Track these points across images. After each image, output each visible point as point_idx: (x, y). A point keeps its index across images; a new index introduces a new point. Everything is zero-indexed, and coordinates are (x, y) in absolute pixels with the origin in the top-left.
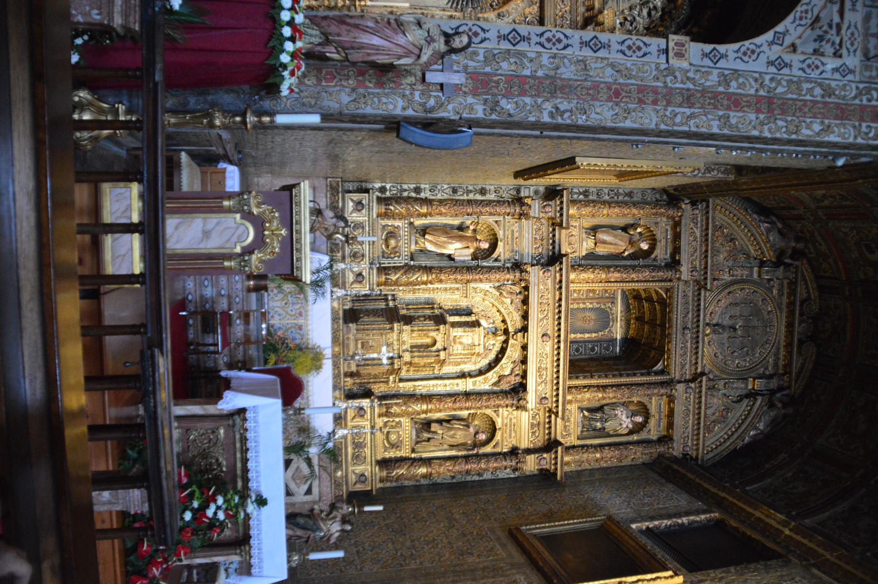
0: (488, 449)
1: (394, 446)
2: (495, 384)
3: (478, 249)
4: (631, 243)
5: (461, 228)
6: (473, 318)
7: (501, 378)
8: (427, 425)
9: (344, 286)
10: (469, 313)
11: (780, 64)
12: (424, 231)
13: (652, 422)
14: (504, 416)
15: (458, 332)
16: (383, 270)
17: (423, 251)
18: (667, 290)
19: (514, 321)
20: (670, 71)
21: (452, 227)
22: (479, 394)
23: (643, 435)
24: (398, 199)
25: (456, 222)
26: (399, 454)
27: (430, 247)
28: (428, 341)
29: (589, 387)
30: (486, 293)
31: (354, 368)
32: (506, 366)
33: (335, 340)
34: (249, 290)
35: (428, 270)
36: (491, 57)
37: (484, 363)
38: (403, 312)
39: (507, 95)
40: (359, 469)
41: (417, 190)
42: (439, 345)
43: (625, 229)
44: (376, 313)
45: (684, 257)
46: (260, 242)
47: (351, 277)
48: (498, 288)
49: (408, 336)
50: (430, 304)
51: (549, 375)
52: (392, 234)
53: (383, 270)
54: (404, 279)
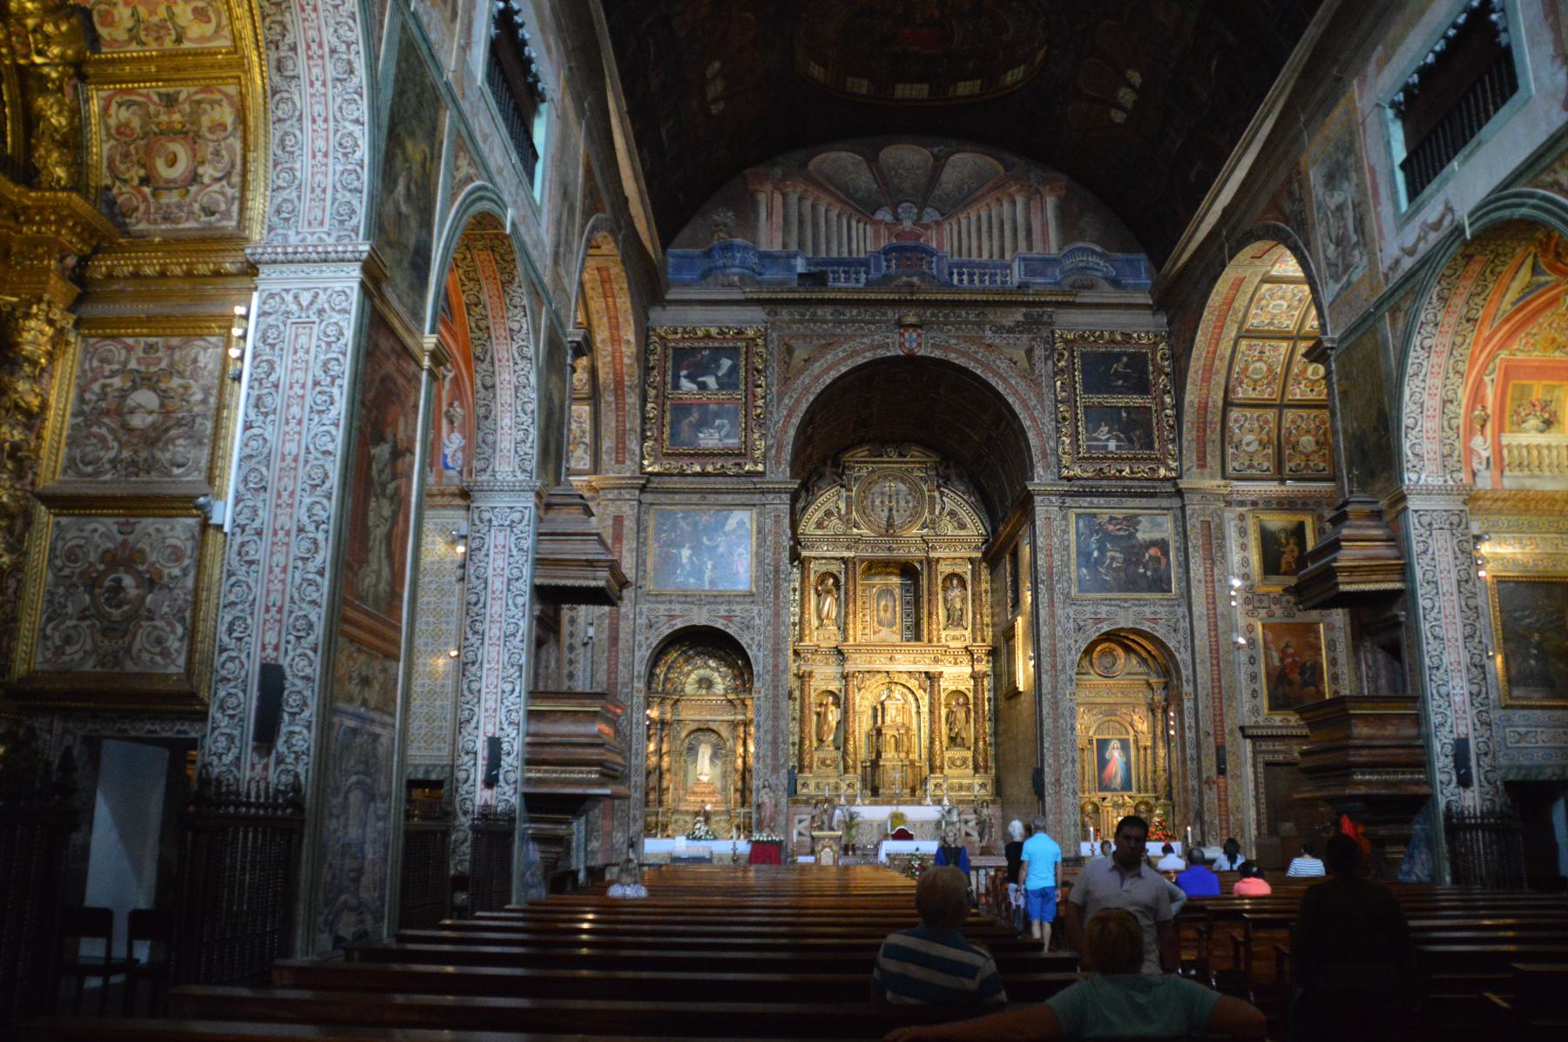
0: (971, 695)
1: (964, 761)
2: (925, 691)
3: (833, 704)
4: (828, 592)
5: (818, 714)
6: (879, 707)
7: (920, 687)
8: (952, 740)
9: (856, 796)
10: (875, 709)
11: (759, 645)
12: (821, 741)
13: (958, 570)
14: (946, 685)
15: (888, 720)
16: (846, 770)
17: (834, 740)
18: (863, 561)
19: (882, 678)
20: (766, 696)
21: (818, 720)
22: (931, 704)
23: (968, 578)
24: (801, 759)
25: (815, 717)
26: (971, 759)
27: (831, 738)
28: (893, 740)
29: (929, 625)
30: (862, 698)
31: (908, 791)
32: (913, 684)
33: (889, 803)
34: (854, 854)
35: (846, 740)
36: (766, 767)
37: (910, 698)
38: (874, 756)
39: (778, 760)
40: (977, 788)
41: (794, 744)
42: (896, 733)
43: (819, 595)
44: (873, 775)
45: (838, 555)
46: (830, 847)
47: (850, 791)
48: (859, 689)
49: (889, 755)
50: (869, 736)
51: (919, 657)
52: (823, 762)
53: (846, 770)
54: (852, 756)
